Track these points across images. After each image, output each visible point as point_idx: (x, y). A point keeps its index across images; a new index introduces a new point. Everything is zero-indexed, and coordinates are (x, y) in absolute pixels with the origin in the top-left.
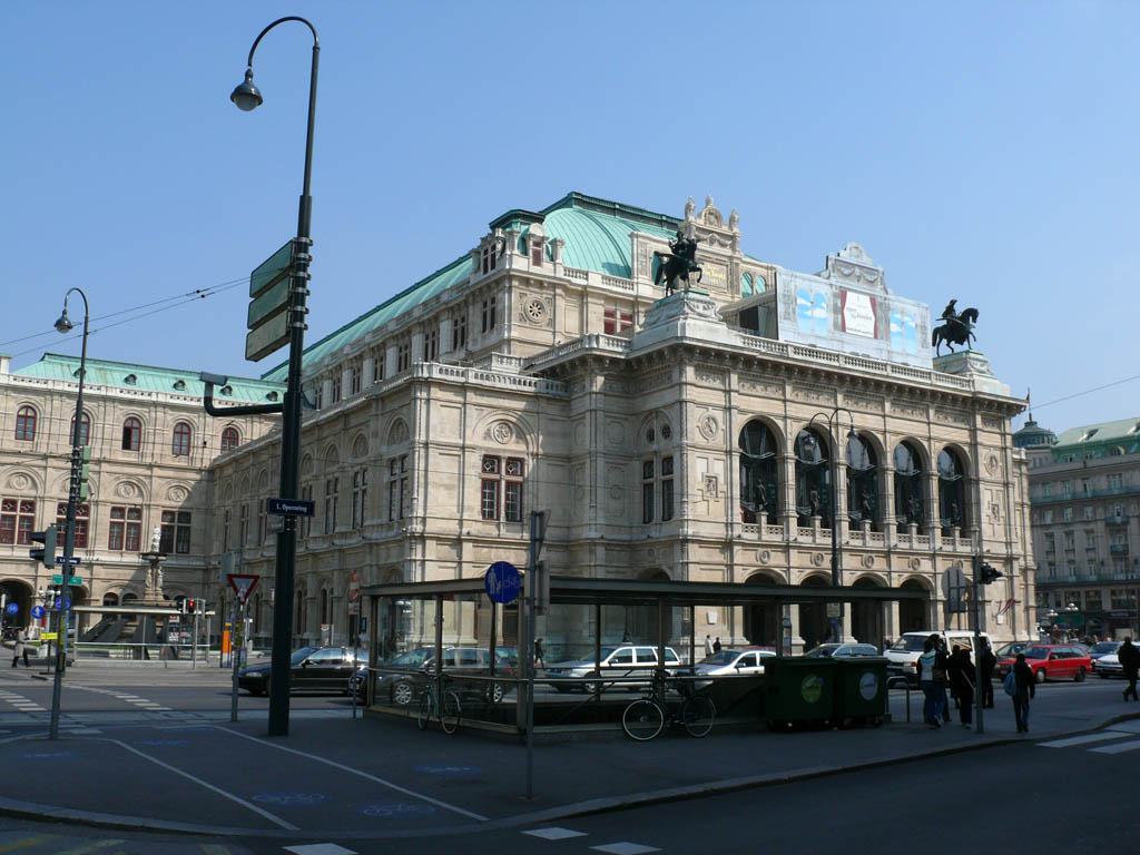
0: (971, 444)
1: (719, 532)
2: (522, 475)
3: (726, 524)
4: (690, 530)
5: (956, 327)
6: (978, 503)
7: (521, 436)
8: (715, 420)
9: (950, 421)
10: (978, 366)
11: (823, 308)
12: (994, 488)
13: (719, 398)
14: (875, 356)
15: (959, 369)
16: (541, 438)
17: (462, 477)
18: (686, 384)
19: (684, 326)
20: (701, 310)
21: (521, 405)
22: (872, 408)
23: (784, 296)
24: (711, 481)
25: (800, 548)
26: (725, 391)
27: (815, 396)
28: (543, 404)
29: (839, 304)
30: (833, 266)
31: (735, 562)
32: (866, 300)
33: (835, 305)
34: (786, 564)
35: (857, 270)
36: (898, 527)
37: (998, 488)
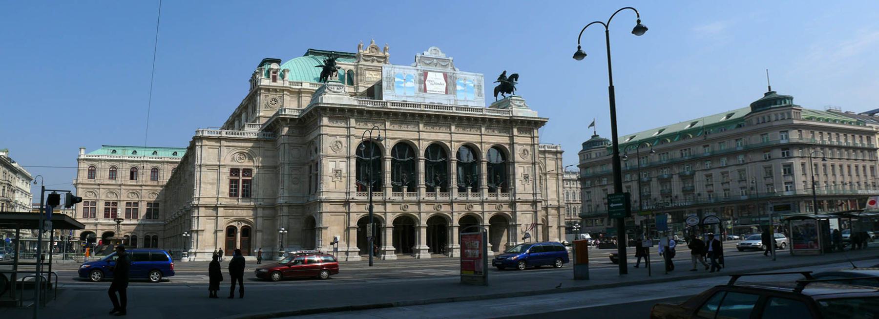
0: (510, 144)
1: (343, 197)
2: (251, 176)
3: (346, 193)
4: (324, 196)
5: (506, 85)
6: (514, 174)
7: (251, 158)
8: (340, 142)
9: (496, 132)
10: (518, 103)
11: (412, 82)
12: (526, 166)
13: (344, 132)
14: (445, 103)
15: (506, 106)
16: (261, 159)
17: (219, 180)
18: (323, 126)
19: (322, 99)
20: (336, 90)
21: (251, 145)
22: (443, 129)
23: (387, 78)
24: (337, 172)
25: (393, 202)
26: (347, 128)
27: (406, 126)
28: (262, 143)
29: (422, 78)
30: (419, 60)
31: (351, 211)
32: (441, 76)
33: (420, 80)
34: (384, 211)
35: (435, 60)
36: (458, 189)
37: (528, 166)
